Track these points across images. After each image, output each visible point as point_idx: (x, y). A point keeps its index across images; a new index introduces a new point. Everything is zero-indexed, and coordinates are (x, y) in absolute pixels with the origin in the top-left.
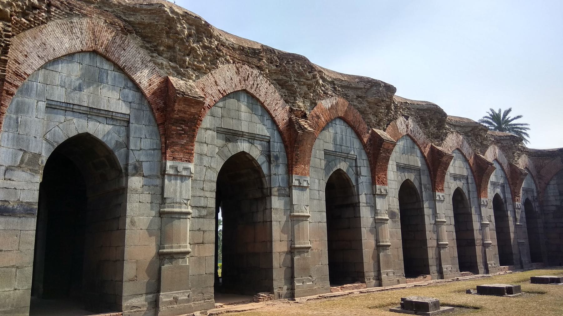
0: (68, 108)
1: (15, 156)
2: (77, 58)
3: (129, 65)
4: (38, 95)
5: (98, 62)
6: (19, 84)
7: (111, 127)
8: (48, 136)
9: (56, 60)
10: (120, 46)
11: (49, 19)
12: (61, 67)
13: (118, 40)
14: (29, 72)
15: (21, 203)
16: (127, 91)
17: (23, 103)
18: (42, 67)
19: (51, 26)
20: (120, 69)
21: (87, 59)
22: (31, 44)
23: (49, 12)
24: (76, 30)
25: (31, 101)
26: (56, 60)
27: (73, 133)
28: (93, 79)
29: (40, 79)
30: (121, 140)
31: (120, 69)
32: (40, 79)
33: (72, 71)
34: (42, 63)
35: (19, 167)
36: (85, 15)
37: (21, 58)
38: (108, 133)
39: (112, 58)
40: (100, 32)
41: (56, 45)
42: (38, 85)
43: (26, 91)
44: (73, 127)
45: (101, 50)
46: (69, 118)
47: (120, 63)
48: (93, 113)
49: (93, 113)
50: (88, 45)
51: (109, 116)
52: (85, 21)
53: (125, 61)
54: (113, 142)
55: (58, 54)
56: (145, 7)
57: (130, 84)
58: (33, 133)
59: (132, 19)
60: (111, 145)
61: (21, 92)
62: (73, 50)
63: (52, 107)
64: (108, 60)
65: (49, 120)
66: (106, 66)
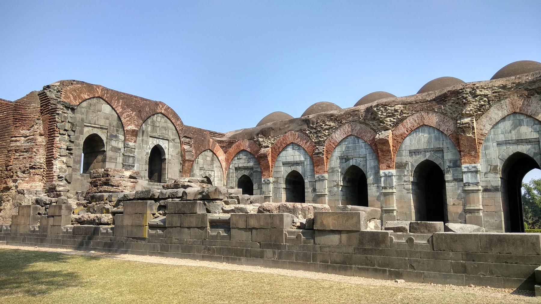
0: (507, 143)
1: (487, 168)
2: (507, 118)
3: (534, 113)
4: (492, 140)
5: (518, 117)
6: (483, 138)
7: (530, 146)
8: (500, 157)
9: (497, 123)
10: (527, 105)
11: (490, 106)
12: (501, 125)
13: (526, 103)
14: (487, 132)
15: (493, 187)
16: (535, 126)
17: (487, 146)
18: (492, 128)
19: (492, 109)
20: (530, 116)
21: (512, 117)
22: (485, 120)
23: (489, 104)
24: (504, 106)
25: (490, 144)
26: (497, 123)
27: (511, 153)
28: (517, 125)
29: (492, 133)
30: (536, 151)
31: (530, 116)
32: (492, 133)
33: (508, 124)
34: (491, 126)
35: (490, 172)
36: (506, 98)
37: (482, 128)
38: (529, 149)
39: (524, 112)
40: (515, 102)
41: (496, 117)
42: (492, 136)
43: (487, 140)
44: (511, 151)
45: (518, 111)
46: (508, 147)
47: (528, 114)
48: (519, 142)
49: (519, 142)
50: (512, 110)
51: (528, 141)
52: (507, 100)
53: (531, 112)
54: (532, 154)
55: (497, 121)
56: (538, 79)
57: (536, 122)
58: (493, 157)
59: (534, 87)
60: (531, 155)
61: (485, 141)
62: (504, 116)
63: (499, 144)
64: (522, 114)
65: (499, 150)
66: (522, 117)
